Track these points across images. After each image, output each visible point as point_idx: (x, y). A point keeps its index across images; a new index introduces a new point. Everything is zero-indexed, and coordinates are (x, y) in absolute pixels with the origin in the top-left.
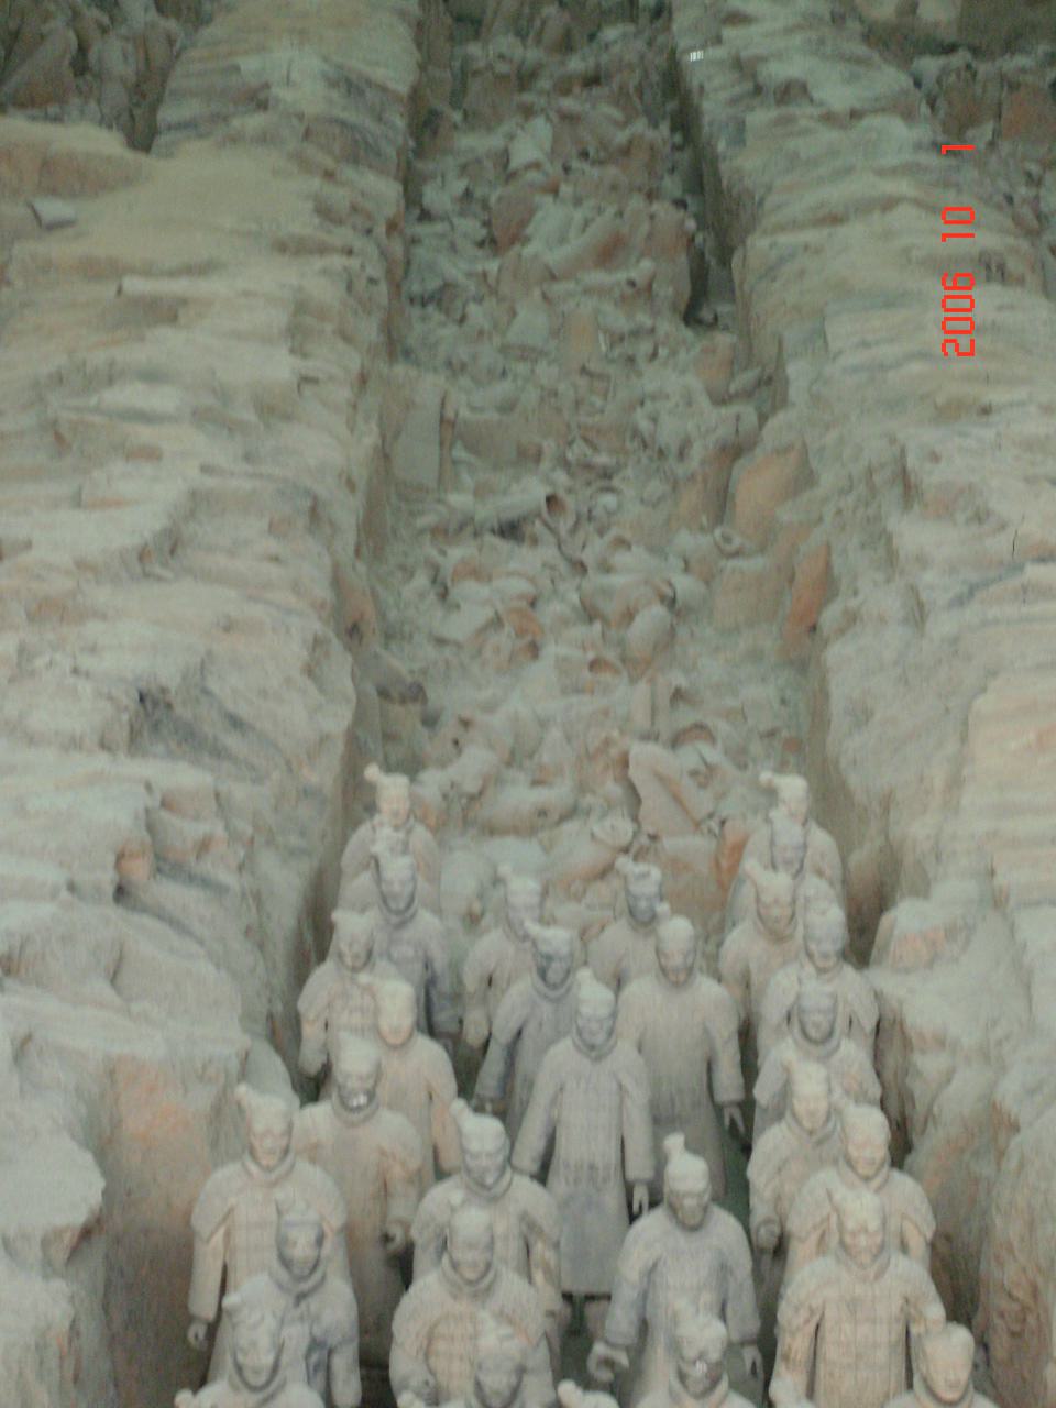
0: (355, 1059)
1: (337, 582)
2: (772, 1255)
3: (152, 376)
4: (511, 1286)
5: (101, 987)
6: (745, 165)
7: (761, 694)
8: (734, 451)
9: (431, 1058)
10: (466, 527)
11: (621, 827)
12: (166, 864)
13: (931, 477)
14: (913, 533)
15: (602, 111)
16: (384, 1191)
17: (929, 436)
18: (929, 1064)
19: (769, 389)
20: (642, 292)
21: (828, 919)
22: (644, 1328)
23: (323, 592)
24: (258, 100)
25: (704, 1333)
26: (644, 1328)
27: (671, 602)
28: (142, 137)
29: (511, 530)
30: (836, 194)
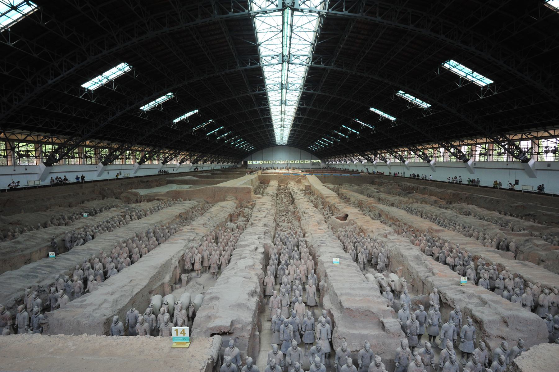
0: (277, 243)
2: (300, 253)
6: (294, 197)
7: (298, 224)
11: (290, 231)
12: (267, 233)
13: (306, 212)
14: (305, 215)
15: (286, 194)
18: (308, 243)
19: (297, 208)
20: (289, 203)
22: (294, 257)
24: (269, 194)
25: (297, 257)
26: (294, 257)
29: (283, 216)
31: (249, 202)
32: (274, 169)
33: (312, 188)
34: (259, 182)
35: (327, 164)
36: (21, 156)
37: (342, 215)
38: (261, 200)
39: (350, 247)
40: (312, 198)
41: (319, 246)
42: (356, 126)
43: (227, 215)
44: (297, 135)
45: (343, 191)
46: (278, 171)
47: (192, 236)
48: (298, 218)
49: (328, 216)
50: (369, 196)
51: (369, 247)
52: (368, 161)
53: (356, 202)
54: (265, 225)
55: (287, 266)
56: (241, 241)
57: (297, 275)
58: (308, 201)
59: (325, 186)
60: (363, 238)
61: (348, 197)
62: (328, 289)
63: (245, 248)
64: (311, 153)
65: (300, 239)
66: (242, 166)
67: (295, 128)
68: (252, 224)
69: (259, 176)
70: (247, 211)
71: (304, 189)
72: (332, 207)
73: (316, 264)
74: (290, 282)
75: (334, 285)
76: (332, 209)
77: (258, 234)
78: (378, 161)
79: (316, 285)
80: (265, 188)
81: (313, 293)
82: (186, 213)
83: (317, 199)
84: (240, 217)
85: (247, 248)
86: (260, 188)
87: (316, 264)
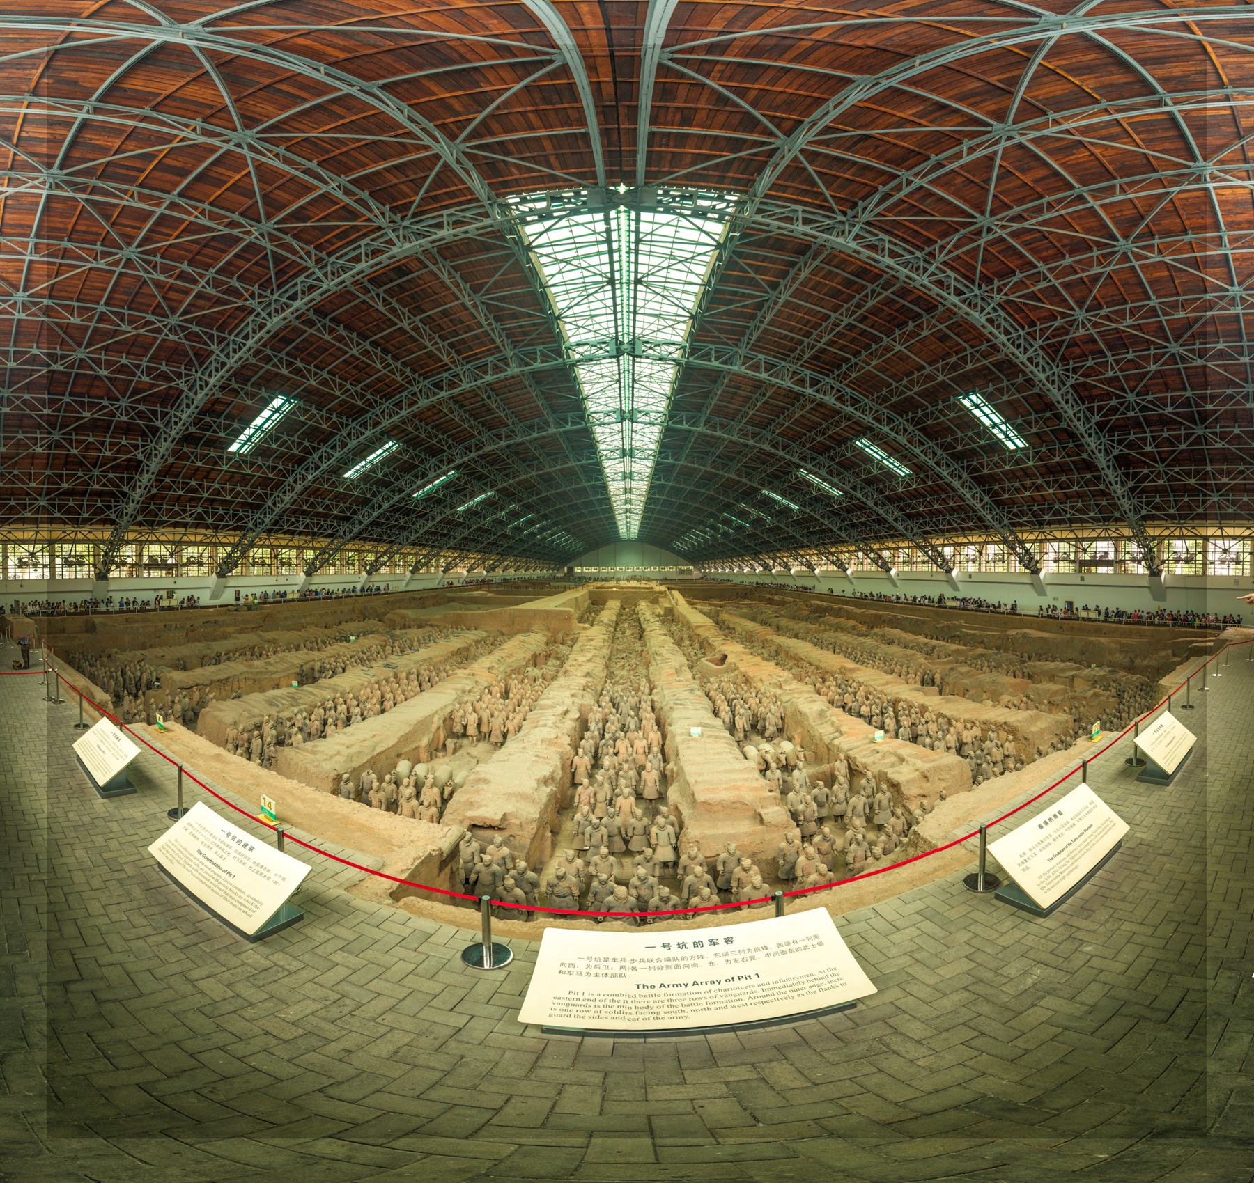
2: (641, 720)
7: (644, 671)
21: (647, 691)
36: (283, 564)
37: (718, 656)
38: (589, 633)
40: (674, 628)
42: (743, 514)
43: (528, 655)
45: (724, 616)
47: (468, 684)
50: (763, 623)
51: (754, 706)
52: (765, 568)
54: (588, 674)
55: (615, 740)
65: (644, 697)
68: (566, 671)
69: (590, 592)
73: (664, 737)
75: (687, 769)
76: (704, 645)
78: (778, 568)
80: (598, 612)
82: (467, 649)
85: (550, 712)
87: (664, 737)
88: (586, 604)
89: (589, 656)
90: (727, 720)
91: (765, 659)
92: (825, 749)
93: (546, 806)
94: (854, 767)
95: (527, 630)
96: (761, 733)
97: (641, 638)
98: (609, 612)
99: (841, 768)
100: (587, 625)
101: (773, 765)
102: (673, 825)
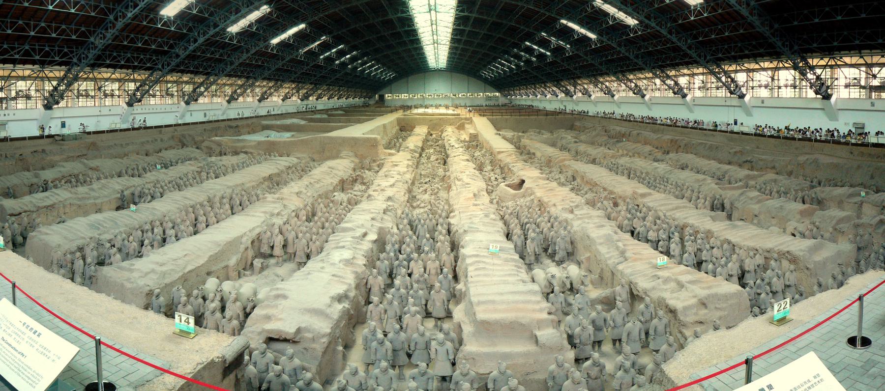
1: (408, 187)
3: (394, 171)
4: (412, 245)
5: (380, 220)
6: (449, 152)
8: (445, 176)
9: (408, 227)
10: (422, 183)
13: (459, 178)
14: (457, 182)
15: (438, 148)
16: (403, 238)
17: (460, 175)
18: (452, 226)
20: (439, 163)
21: (444, 214)
23: (406, 188)
24: (408, 148)
27: (438, 188)
28: (398, 152)
30: (456, 154)
31: (374, 161)
32: (426, 107)
33: (480, 138)
34: (397, 128)
35: (510, 100)
38: (394, 158)
39: (517, 231)
40: (477, 154)
41: (465, 231)
43: (336, 181)
44: (460, 55)
45: (525, 141)
46: (430, 111)
48: (448, 186)
49: (496, 183)
53: (543, 158)
54: (389, 199)
55: (409, 262)
56: (346, 222)
57: (419, 275)
58: (468, 160)
59: (500, 135)
60: (540, 216)
61: (532, 151)
62: (465, 295)
63: (348, 233)
64: (485, 83)
65: (441, 220)
66: (377, 102)
67: (456, 45)
70: (368, 176)
71: (467, 139)
72: (506, 168)
74: (409, 284)
76: (504, 171)
77: (372, 213)
79: (451, 289)
81: (441, 301)
83: (484, 156)
84: (357, 184)
85: (351, 233)
86: (397, 138)
87: (456, 259)
88: (394, 131)
89: (392, 181)
90: (519, 243)
91: (562, 184)
92: (609, 274)
93: (339, 321)
94: (635, 293)
95: (336, 157)
96: (552, 256)
97: (445, 163)
98: (414, 141)
99: (622, 293)
100: (393, 151)
101: (557, 289)
102: (452, 341)
